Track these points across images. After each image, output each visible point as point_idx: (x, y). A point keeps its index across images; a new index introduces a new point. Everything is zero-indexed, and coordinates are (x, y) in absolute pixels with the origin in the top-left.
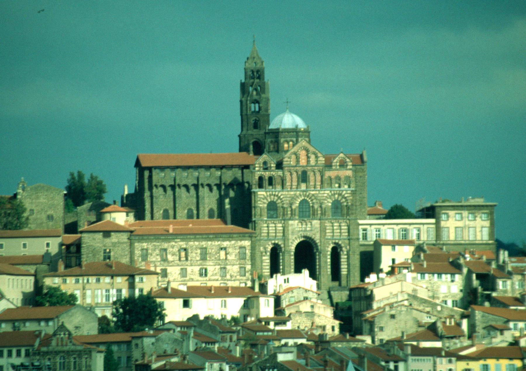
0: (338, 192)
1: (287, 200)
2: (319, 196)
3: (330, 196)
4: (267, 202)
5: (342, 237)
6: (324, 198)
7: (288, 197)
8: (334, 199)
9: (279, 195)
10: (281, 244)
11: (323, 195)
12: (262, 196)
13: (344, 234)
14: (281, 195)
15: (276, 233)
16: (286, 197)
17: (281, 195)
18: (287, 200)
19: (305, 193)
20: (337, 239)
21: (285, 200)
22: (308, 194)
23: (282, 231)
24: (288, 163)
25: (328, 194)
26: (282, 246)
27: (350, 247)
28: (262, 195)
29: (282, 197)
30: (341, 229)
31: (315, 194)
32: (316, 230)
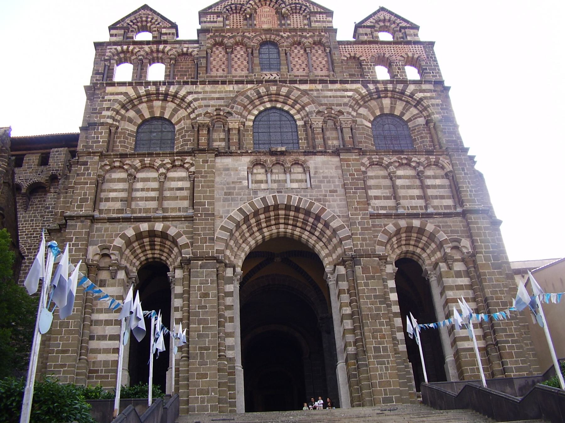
0: (390, 87)
1: (209, 106)
2: (327, 97)
3: (363, 97)
4: (140, 121)
5: (430, 210)
6: (346, 100)
7: (213, 99)
8: (378, 113)
9: (182, 93)
10: (179, 235)
11: (339, 94)
12: (121, 98)
13: (436, 202)
14: (189, 93)
15: (161, 199)
16: (202, 99)
17: (189, 93)
18: (209, 106)
19: (273, 89)
20: (416, 216)
21: (200, 107)
22: (284, 90)
23: (185, 193)
24: (221, 25)
25: (356, 91)
26: (183, 240)
27: (473, 242)
28: (121, 94)
29: (190, 98)
30: (423, 187)
31: (312, 90)
32: (325, 188)
